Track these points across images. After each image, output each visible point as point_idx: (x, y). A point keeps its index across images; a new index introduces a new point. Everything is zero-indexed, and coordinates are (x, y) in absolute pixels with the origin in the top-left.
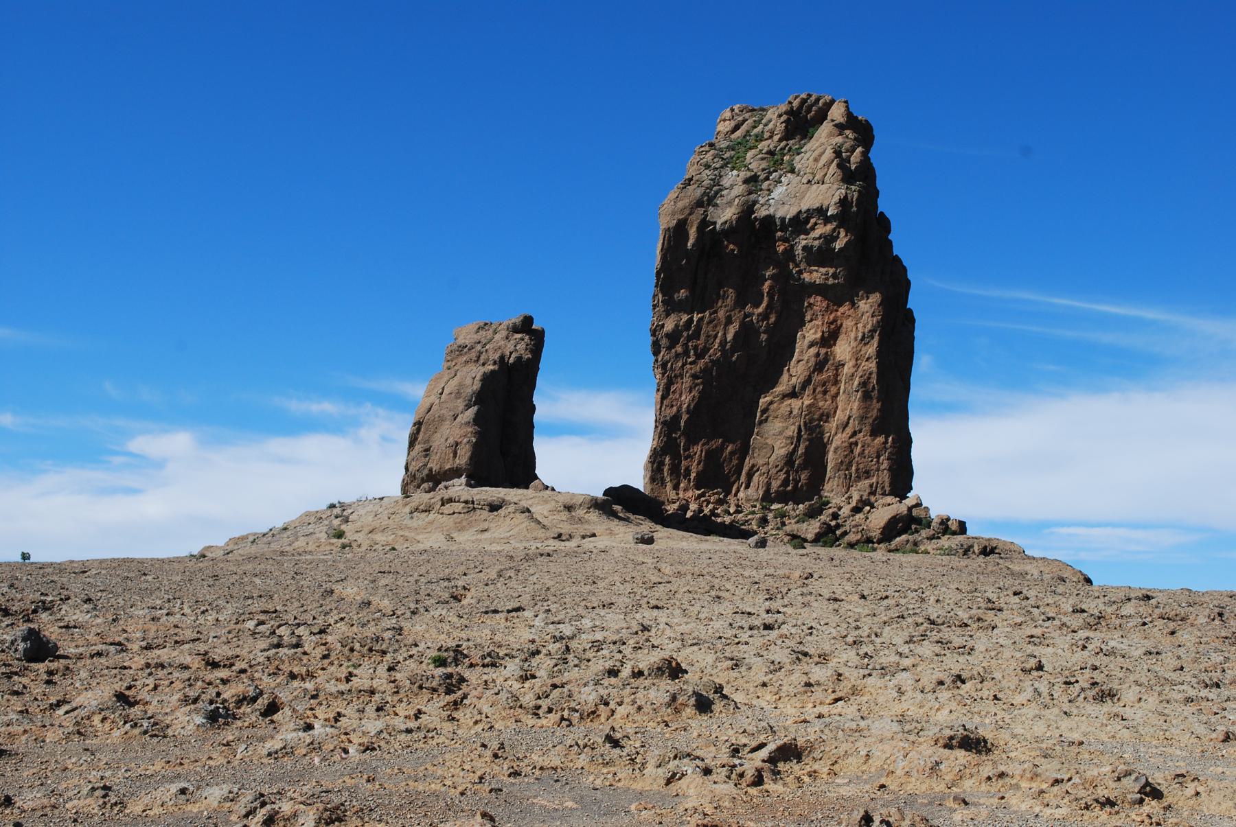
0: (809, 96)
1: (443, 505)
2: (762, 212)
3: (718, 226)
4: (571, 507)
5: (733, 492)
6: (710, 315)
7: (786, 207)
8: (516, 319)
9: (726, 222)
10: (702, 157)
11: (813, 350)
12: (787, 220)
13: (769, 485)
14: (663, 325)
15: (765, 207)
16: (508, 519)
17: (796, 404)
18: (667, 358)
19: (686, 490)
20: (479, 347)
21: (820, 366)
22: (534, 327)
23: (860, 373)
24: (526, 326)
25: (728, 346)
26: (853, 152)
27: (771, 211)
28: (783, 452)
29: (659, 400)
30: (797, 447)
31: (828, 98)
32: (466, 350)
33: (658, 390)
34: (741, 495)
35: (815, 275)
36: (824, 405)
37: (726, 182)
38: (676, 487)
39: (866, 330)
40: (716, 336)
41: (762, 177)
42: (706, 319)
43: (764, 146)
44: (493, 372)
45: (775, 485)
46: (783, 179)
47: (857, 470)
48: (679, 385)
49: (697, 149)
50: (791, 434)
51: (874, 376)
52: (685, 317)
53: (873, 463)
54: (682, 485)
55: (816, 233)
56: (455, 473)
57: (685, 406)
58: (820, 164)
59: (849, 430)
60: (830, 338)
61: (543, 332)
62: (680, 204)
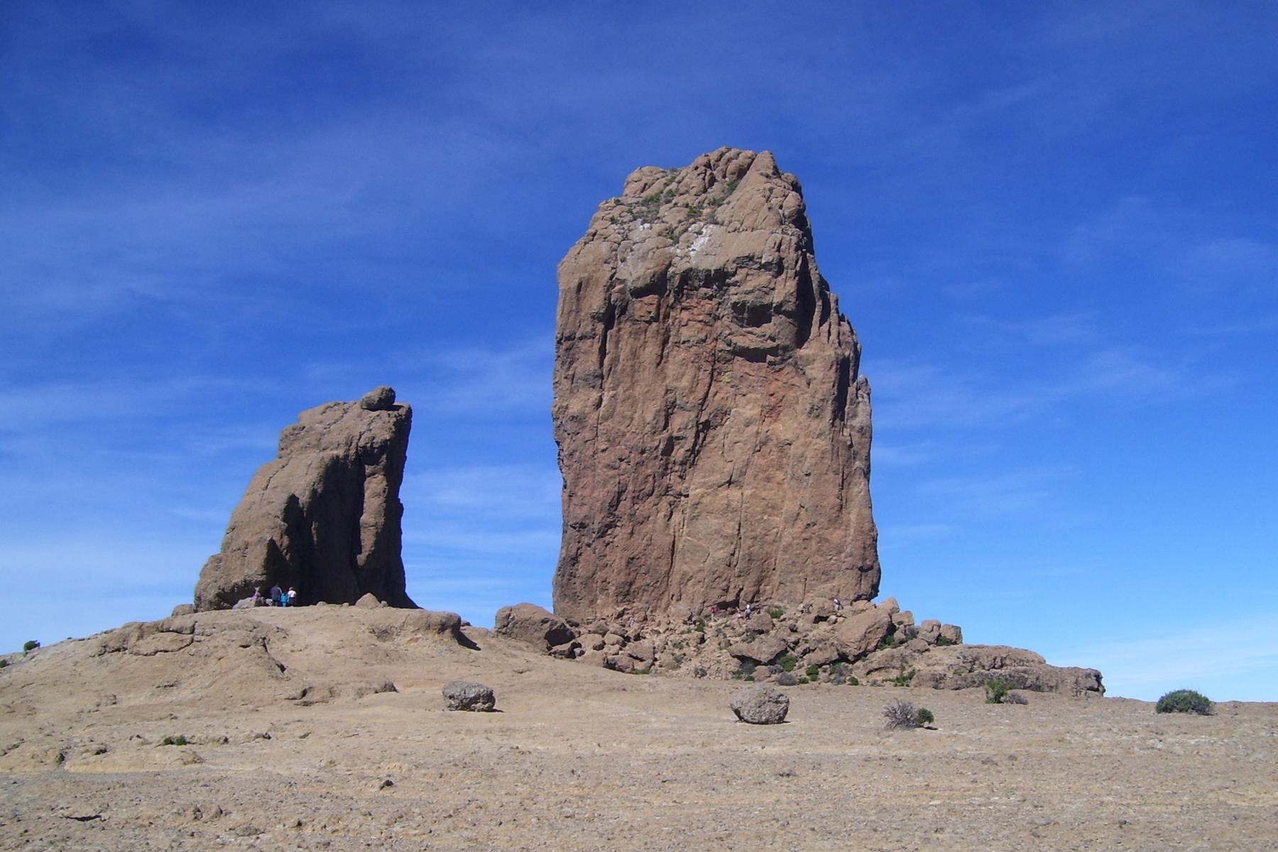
0: (729, 150)
1: (141, 637)
2: (680, 266)
3: (629, 284)
4: (385, 632)
5: (663, 606)
6: (624, 391)
7: (710, 258)
8: (374, 394)
9: (639, 278)
10: (607, 212)
11: (753, 429)
12: (713, 273)
13: (705, 595)
14: (567, 408)
15: (684, 260)
16: (212, 661)
17: (734, 493)
18: (572, 447)
19: (603, 606)
20: (319, 427)
21: (762, 445)
22: (395, 404)
23: (809, 453)
24: (386, 402)
25: (648, 428)
26: (785, 196)
27: (693, 264)
28: (723, 554)
29: (566, 497)
30: (738, 546)
31: (750, 153)
32: (303, 433)
33: (565, 487)
34: (672, 609)
35: (750, 338)
36: (769, 494)
37: (635, 236)
38: (592, 602)
39: (816, 401)
40: (632, 419)
41: (681, 228)
42: (621, 397)
44: (335, 461)
45: (715, 596)
46: (704, 230)
47: (814, 571)
48: (590, 479)
49: (601, 205)
50: (730, 531)
51: (828, 455)
52: (595, 395)
53: (832, 561)
54: (599, 601)
55: (749, 286)
56: (244, 590)
57: (598, 504)
58: (747, 211)
59: (800, 524)
60: (772, 412)
61: (409, 411)
62: (582, 261)
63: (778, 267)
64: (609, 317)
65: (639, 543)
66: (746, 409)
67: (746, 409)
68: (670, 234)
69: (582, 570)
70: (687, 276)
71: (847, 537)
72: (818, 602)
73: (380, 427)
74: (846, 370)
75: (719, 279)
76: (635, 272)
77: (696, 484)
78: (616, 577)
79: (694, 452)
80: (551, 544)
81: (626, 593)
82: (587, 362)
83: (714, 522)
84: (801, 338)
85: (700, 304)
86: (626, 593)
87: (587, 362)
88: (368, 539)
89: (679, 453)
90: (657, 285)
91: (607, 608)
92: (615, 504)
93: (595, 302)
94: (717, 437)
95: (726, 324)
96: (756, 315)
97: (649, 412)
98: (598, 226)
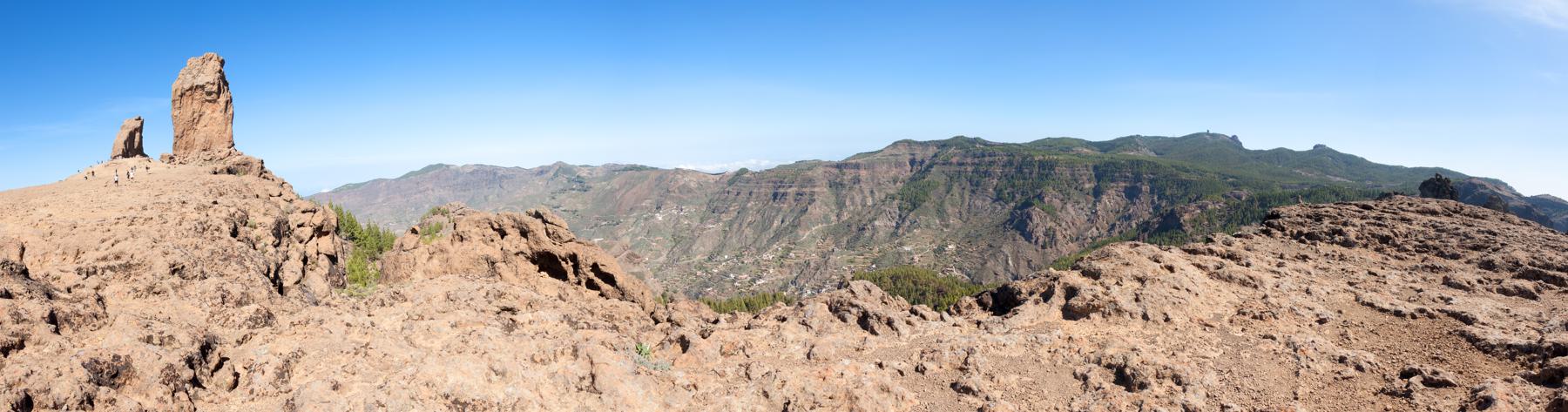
2: (196, 84)
24: (139, 119)
35: (209, 98)
36: (213, 128)
43: (197, 67)
60: (213, 112)
63: (214, 84)
64: (182, 96)
65: (188, 139)
66: (208, 112)
67: (208, 112)
68: (194, 77)
69: (178, 144)
70: (197, 86)
71: (227, 136)
72: (220, 149)
73: (138, 124)
74: (228, 102)
75: (202, 87)
76: (187, 86)
77: (199, 127)
78: (184, 146)
79: (198, 121)
80: (172, 141)
81: (186, 149)
82: (178, 105)
83: (202, 134)
84: (219, 98)
85: (199, 91)
86: (186, 149)
87: (178, 105)
88: (136, 145)
89: (196, 121)
90: (191, 89)
91: (182, 151)
92: (183, 132)
93: (179, 93)
94: (203, 117)
95: (204, 95)
96: (209, 94)
97: (190, 113)
98: (180, 76)
